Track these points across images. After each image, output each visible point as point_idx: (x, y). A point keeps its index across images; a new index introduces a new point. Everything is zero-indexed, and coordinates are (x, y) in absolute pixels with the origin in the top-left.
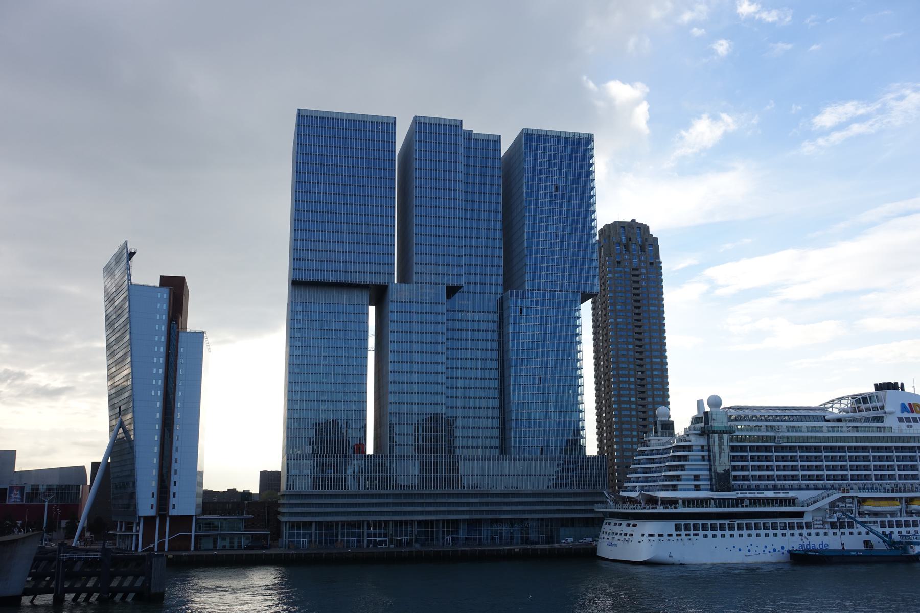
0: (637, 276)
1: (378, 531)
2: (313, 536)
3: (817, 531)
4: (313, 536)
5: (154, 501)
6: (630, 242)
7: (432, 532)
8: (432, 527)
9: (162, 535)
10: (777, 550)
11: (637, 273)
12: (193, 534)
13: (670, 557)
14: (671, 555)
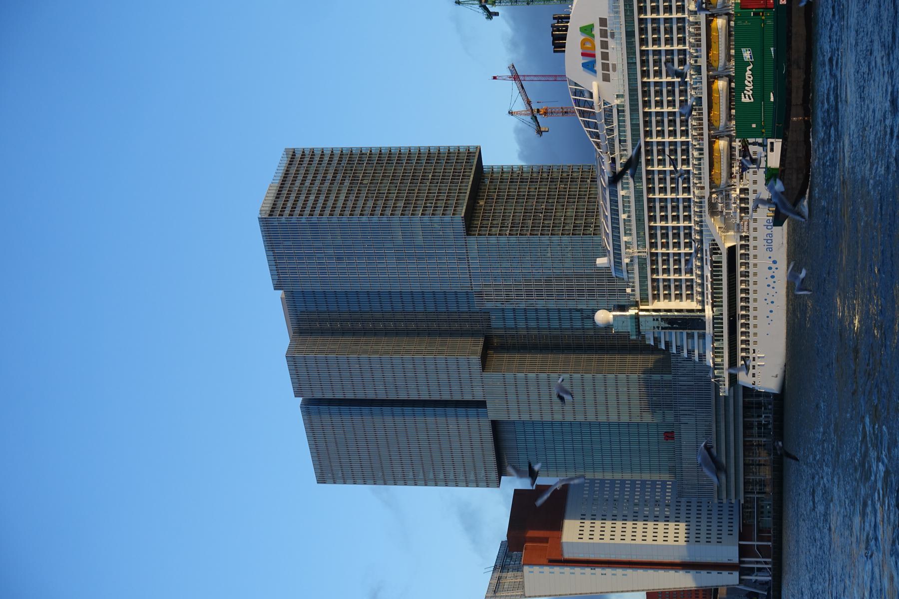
3: (751, 229)
10: (773, 274)
12: (756, 543)
13: (777, 377)
14: (775, 376)
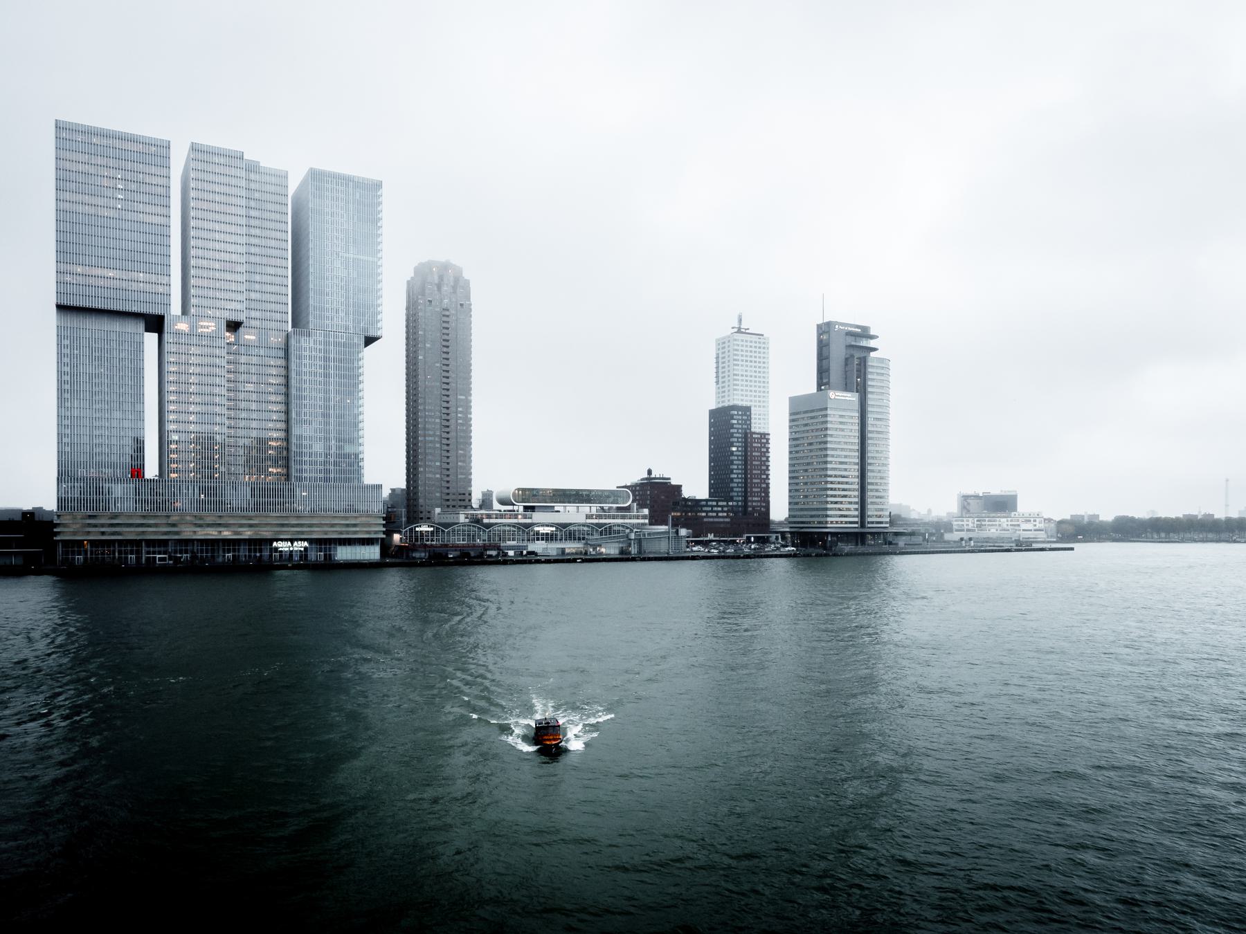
1: (157, 549)
2: (89, 553)
4: (89, 553)
8: (213, 545)
11: (447, 313)
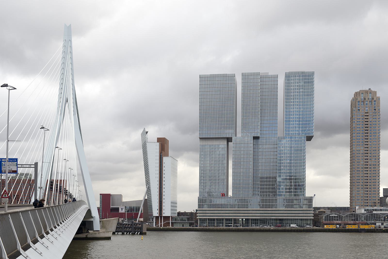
0: (368, 116)
1: (229, 222)
2: (207, 223)
4: (207, 223)
5: (158, 211)
6: (365, 100)
7: (248, 223)
9: (161, 222)
11: (367, 114)
